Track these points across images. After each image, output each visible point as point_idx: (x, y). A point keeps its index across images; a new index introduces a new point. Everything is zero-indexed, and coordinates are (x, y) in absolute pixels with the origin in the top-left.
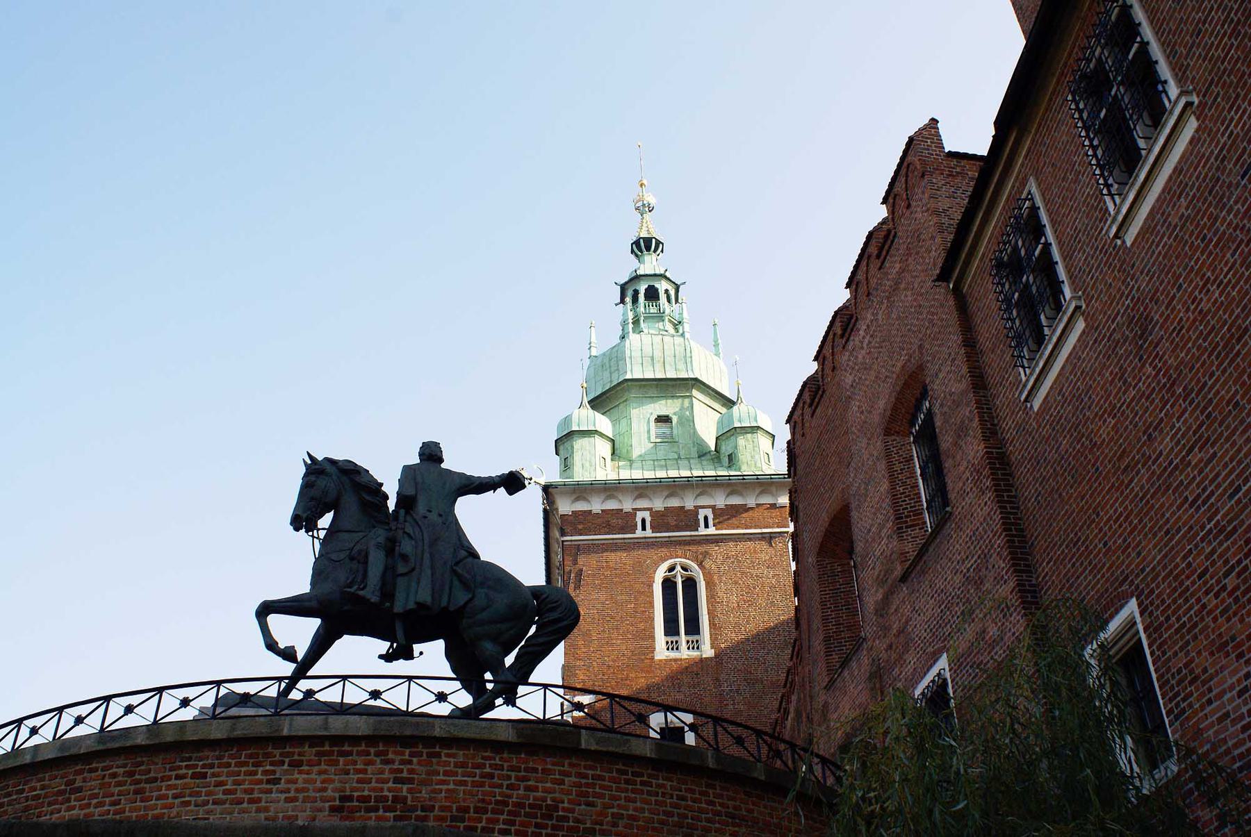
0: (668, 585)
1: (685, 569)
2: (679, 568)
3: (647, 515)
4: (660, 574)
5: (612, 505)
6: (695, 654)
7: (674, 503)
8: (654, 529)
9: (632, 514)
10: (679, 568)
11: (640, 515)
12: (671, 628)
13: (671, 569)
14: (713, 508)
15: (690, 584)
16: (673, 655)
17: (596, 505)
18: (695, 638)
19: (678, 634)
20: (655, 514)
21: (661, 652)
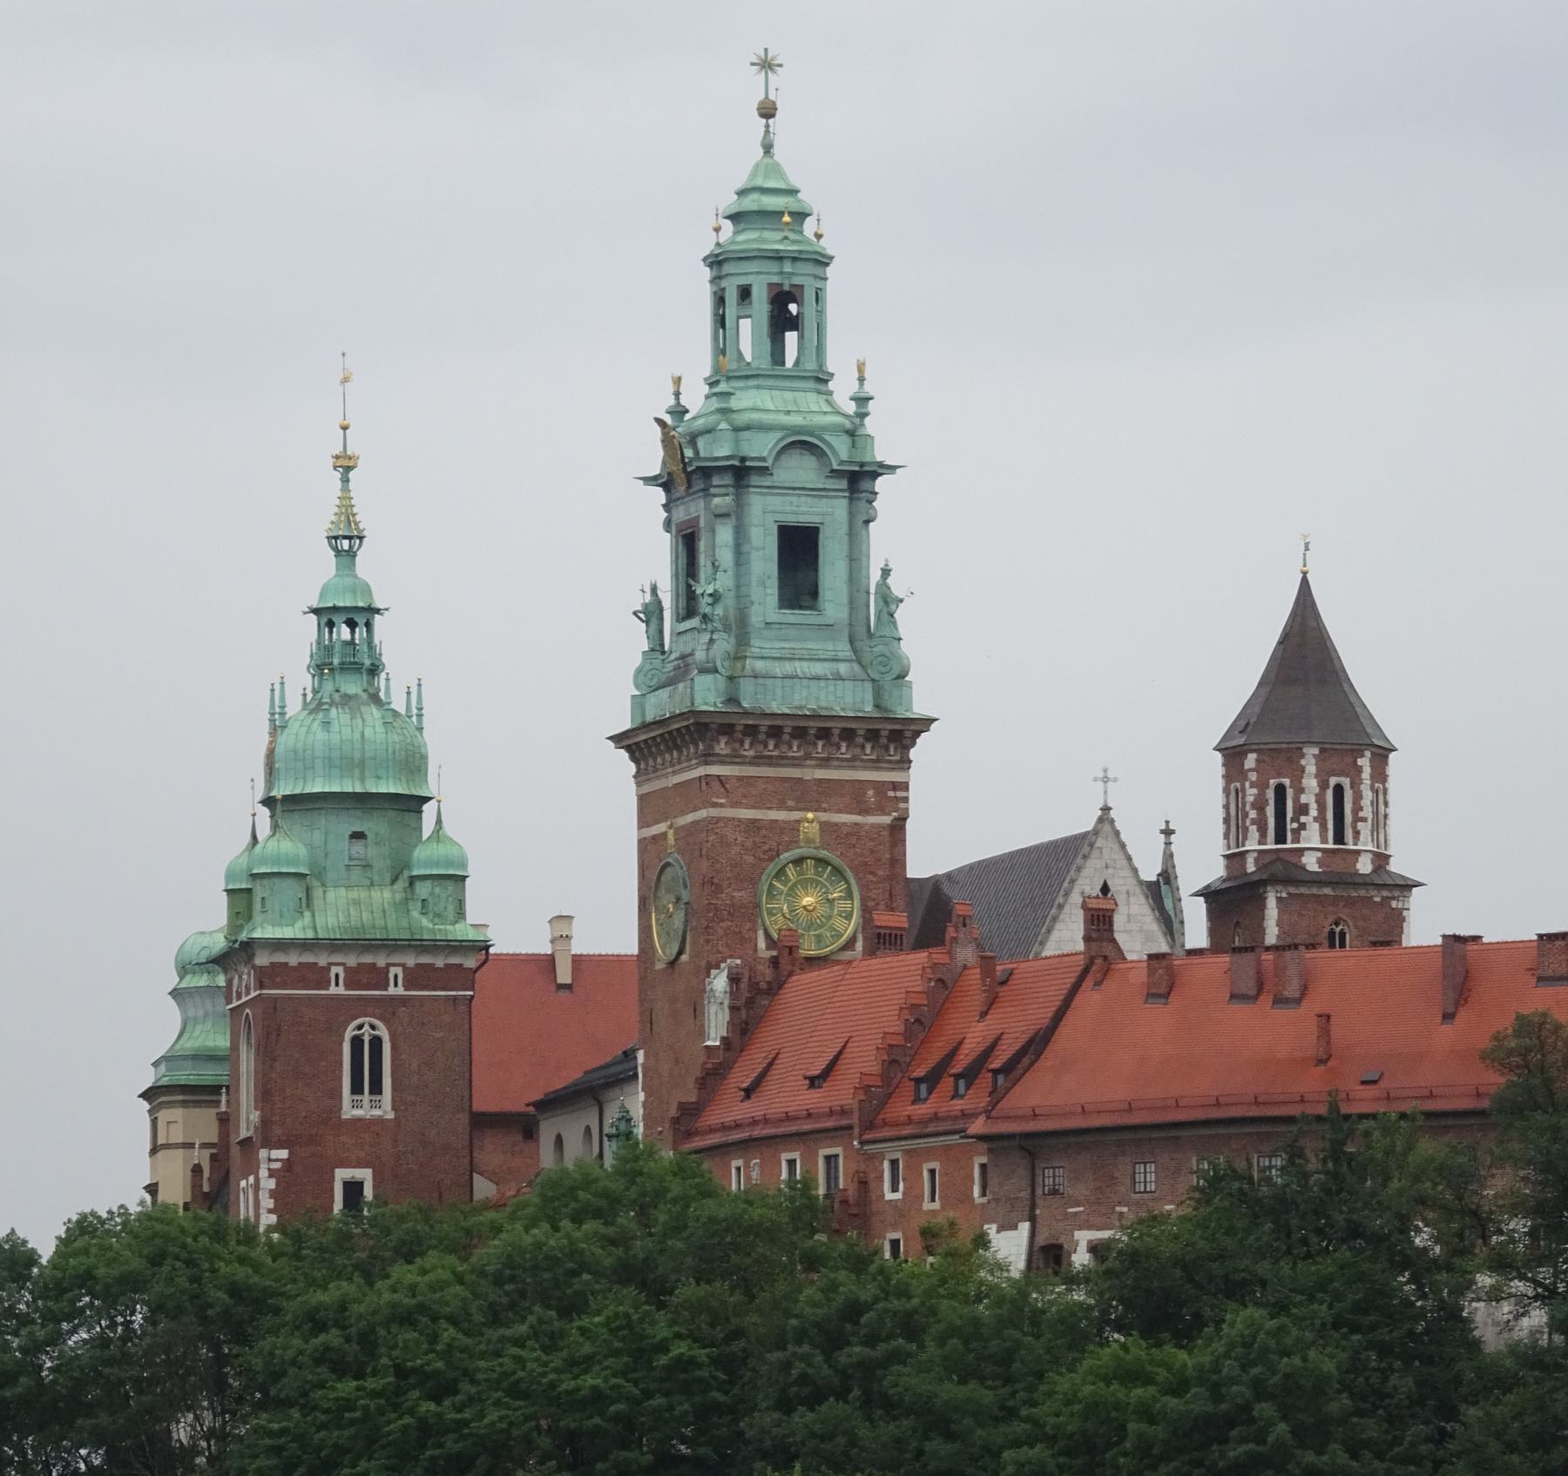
0: (357, 1042)
1: (373, 1027)
2: (366, 1027)
3: (340, 970)
4: (349, 1033)
5: (308, 958)
6: (377, 1112)
7: (367, 959)
8: (347, 987)
9: (327, 969)
10: (366, 1027)
11: (334, 970)
12: (357, 1089)
13: (360, 1027)
14: (403, 965)
15: (376, 1043)
16: (358, 1113)
17: (293, 959)
18: (378, 1098)
19: (362, 1093)
20: (347, 970)
21: (349, 1111)
